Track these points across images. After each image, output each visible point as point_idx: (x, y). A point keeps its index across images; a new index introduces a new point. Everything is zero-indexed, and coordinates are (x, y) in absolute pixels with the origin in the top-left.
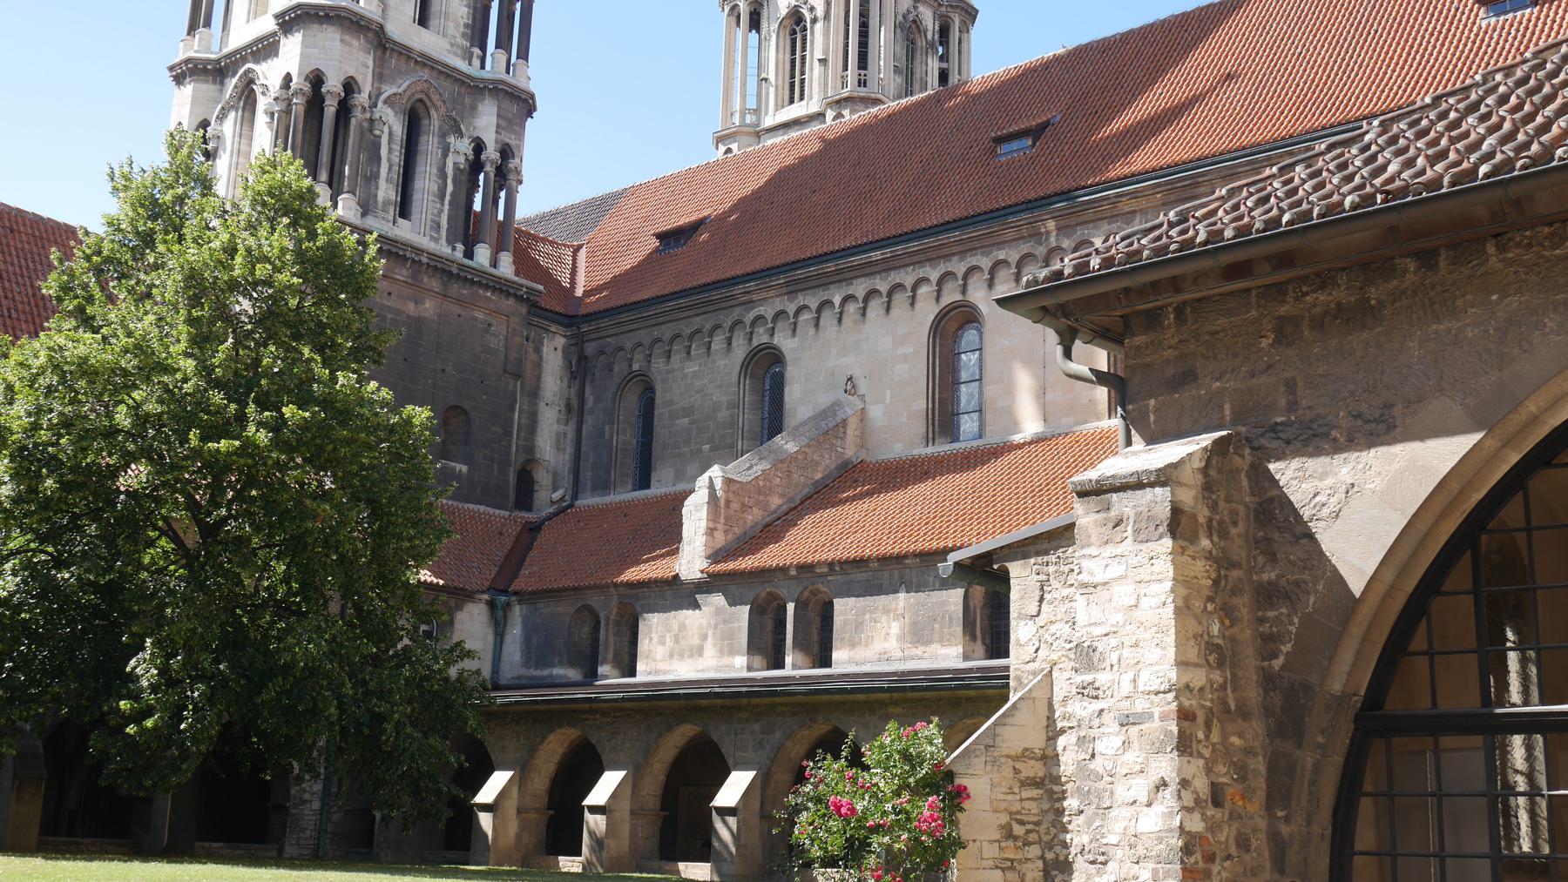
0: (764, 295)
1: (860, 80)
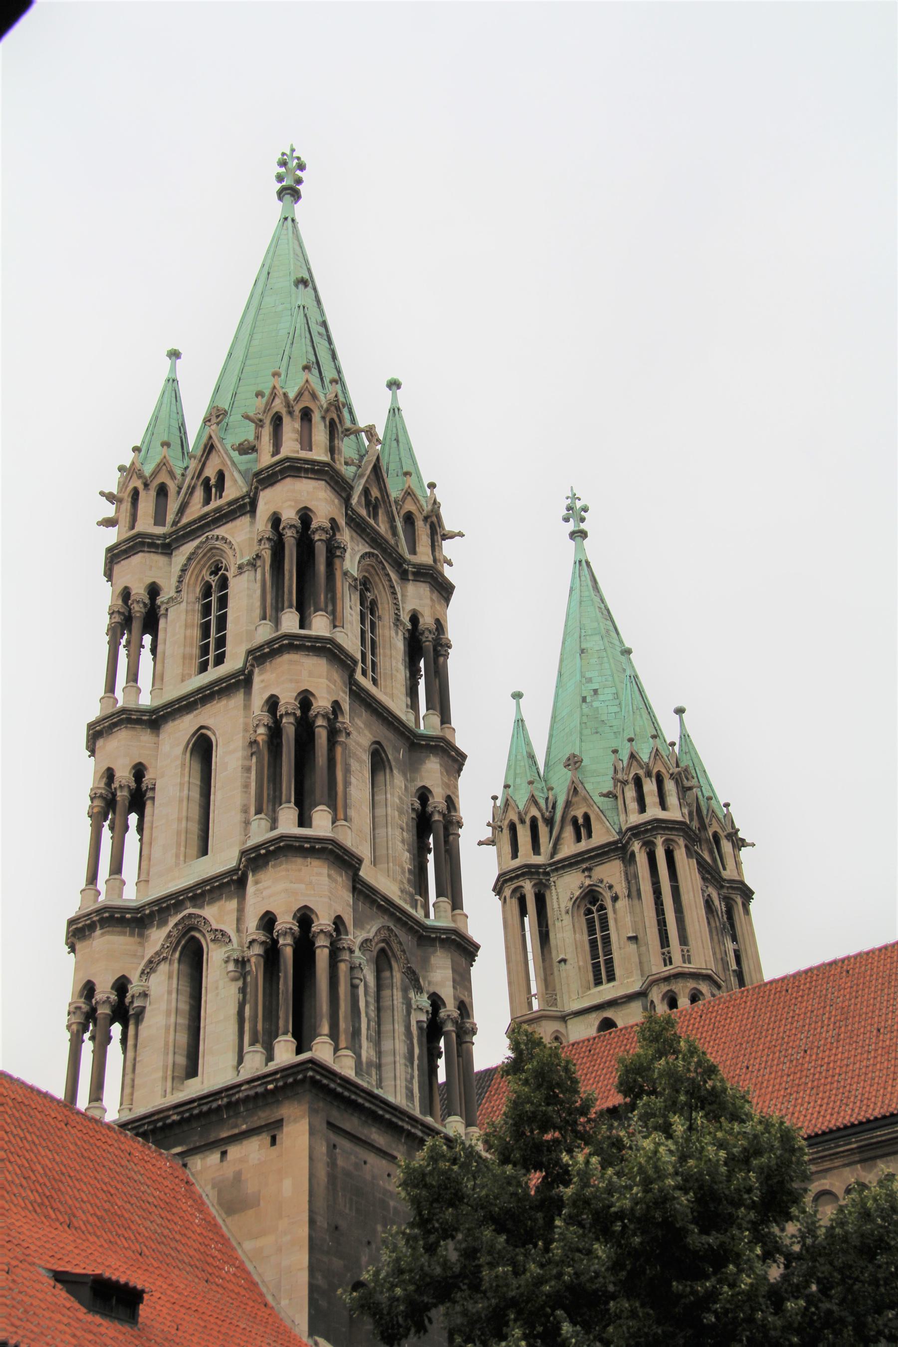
0: (827, 1165)
1: (683, 956)
